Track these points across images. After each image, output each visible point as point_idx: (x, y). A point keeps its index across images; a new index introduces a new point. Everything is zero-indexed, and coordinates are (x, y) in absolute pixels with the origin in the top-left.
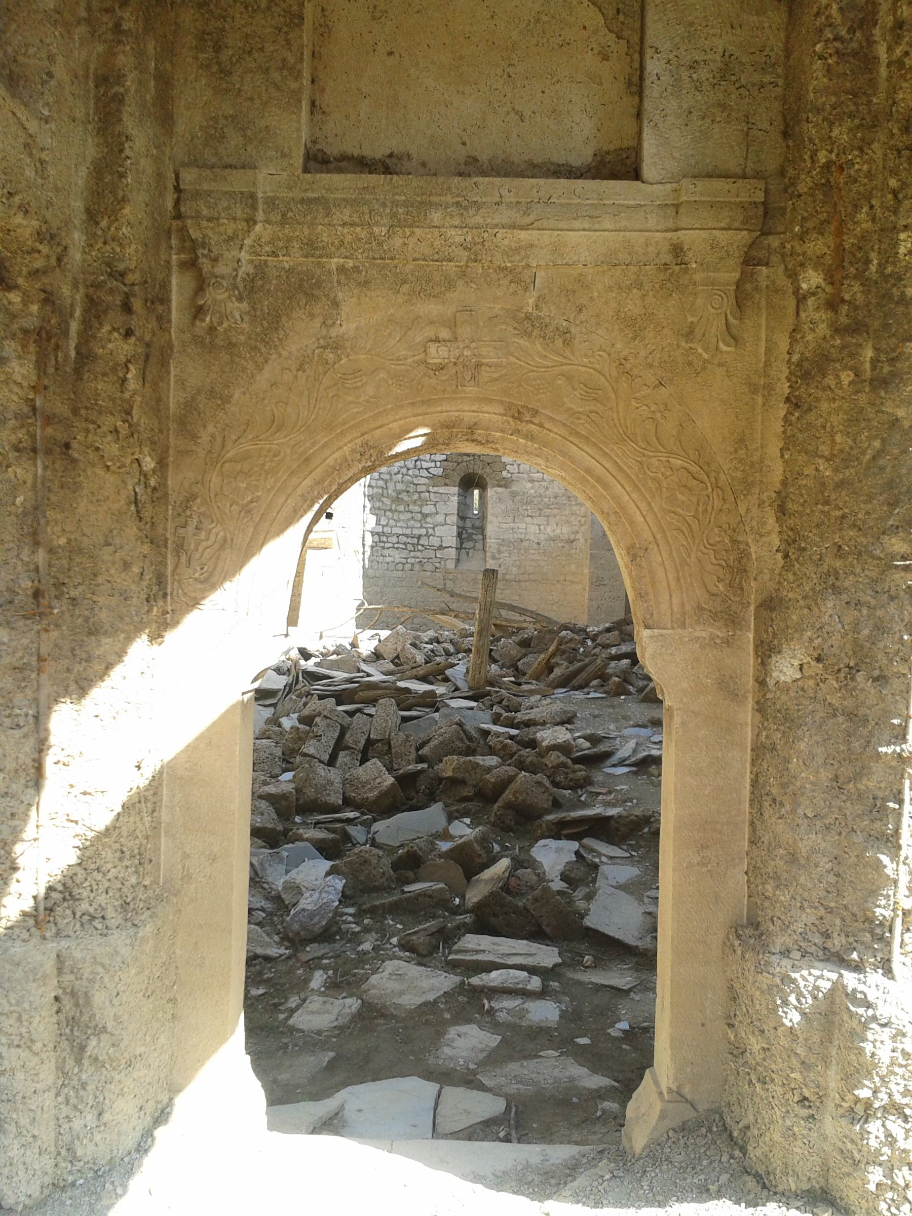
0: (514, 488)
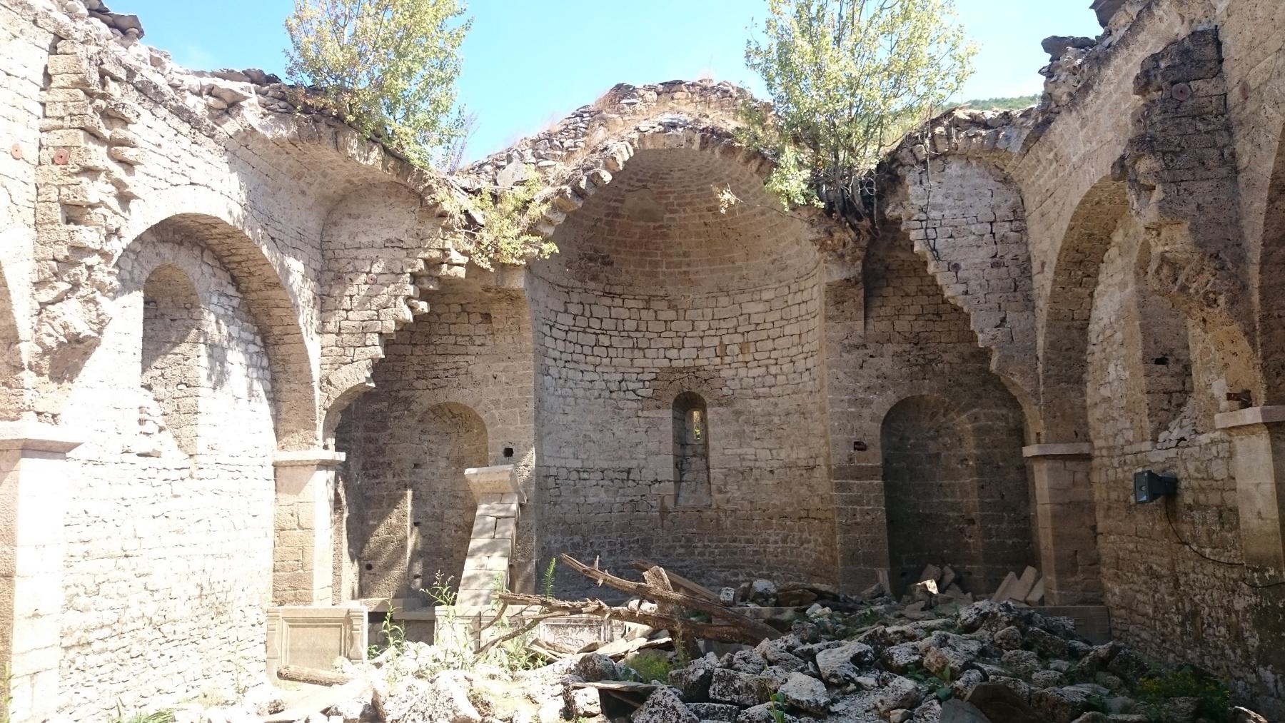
0: (738, 406)
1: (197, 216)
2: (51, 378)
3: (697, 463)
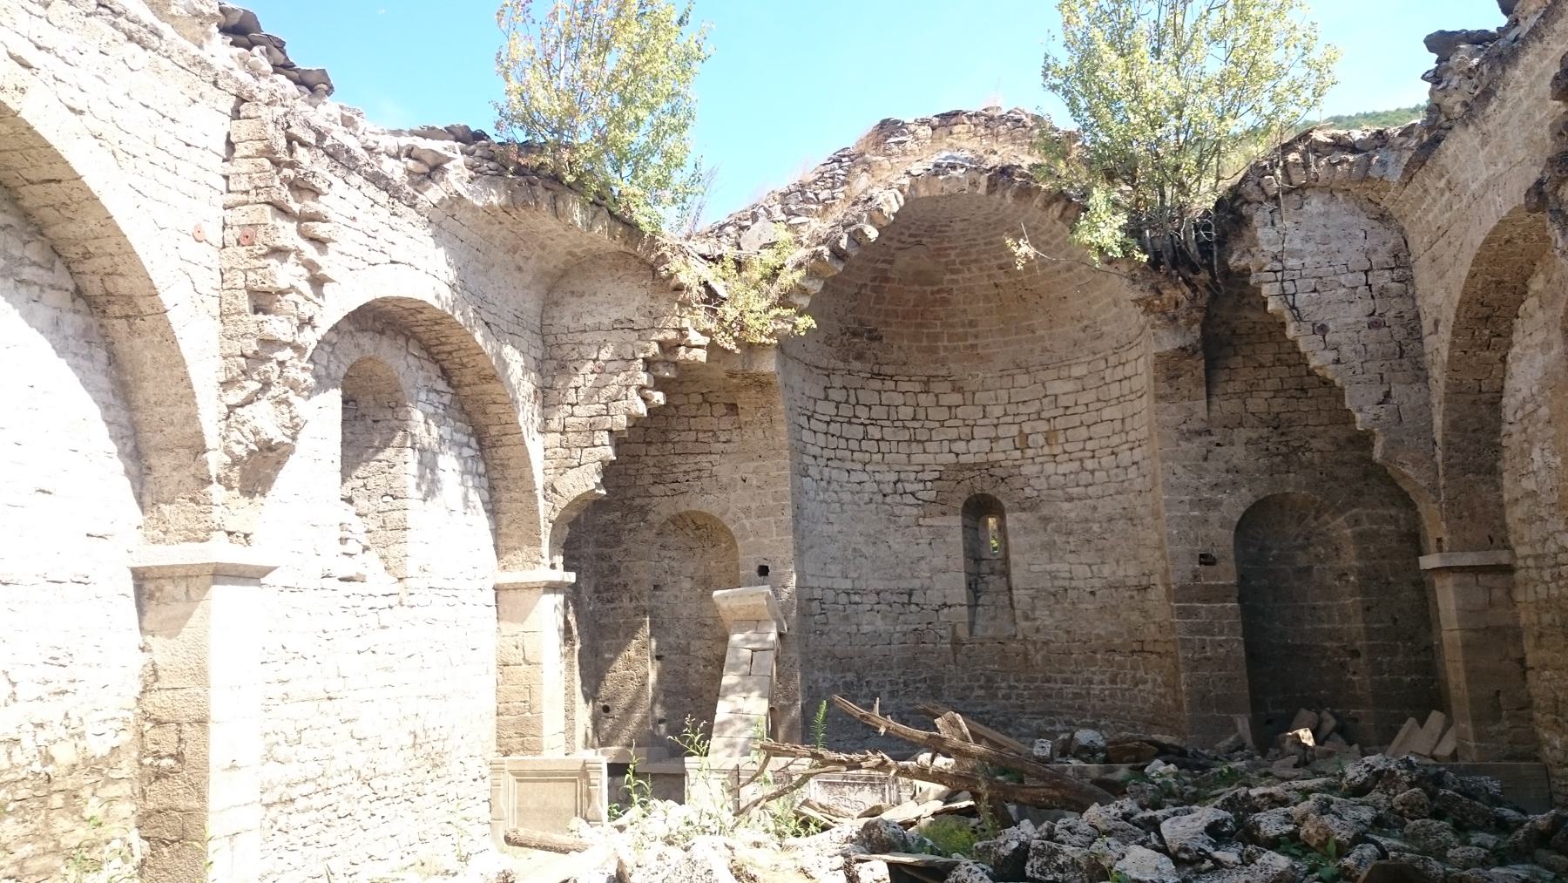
0: (1045, 511)
1: (400, 299)
2: (241, 492)
3: (996, 582)
